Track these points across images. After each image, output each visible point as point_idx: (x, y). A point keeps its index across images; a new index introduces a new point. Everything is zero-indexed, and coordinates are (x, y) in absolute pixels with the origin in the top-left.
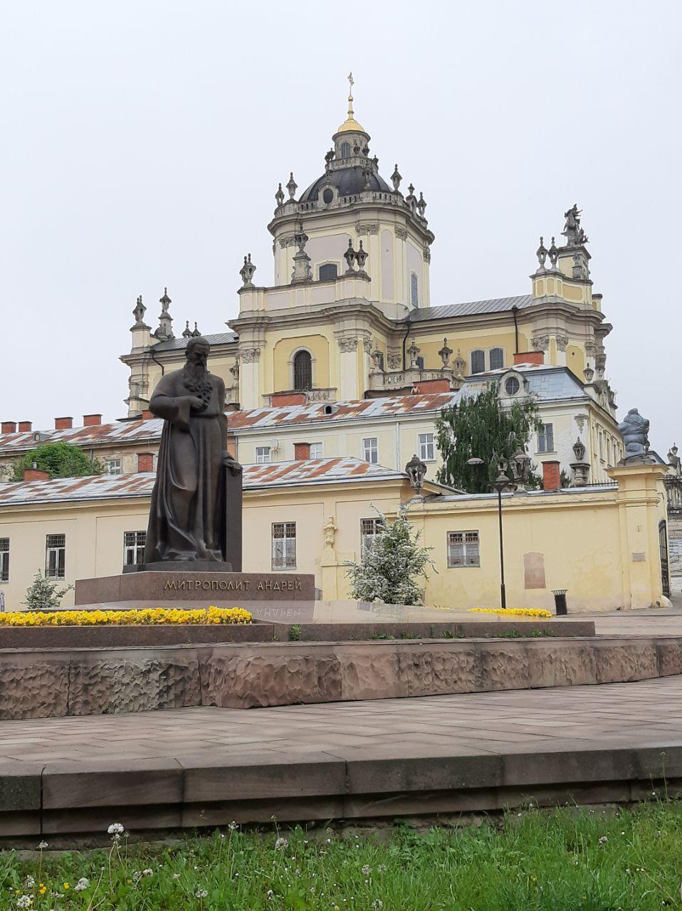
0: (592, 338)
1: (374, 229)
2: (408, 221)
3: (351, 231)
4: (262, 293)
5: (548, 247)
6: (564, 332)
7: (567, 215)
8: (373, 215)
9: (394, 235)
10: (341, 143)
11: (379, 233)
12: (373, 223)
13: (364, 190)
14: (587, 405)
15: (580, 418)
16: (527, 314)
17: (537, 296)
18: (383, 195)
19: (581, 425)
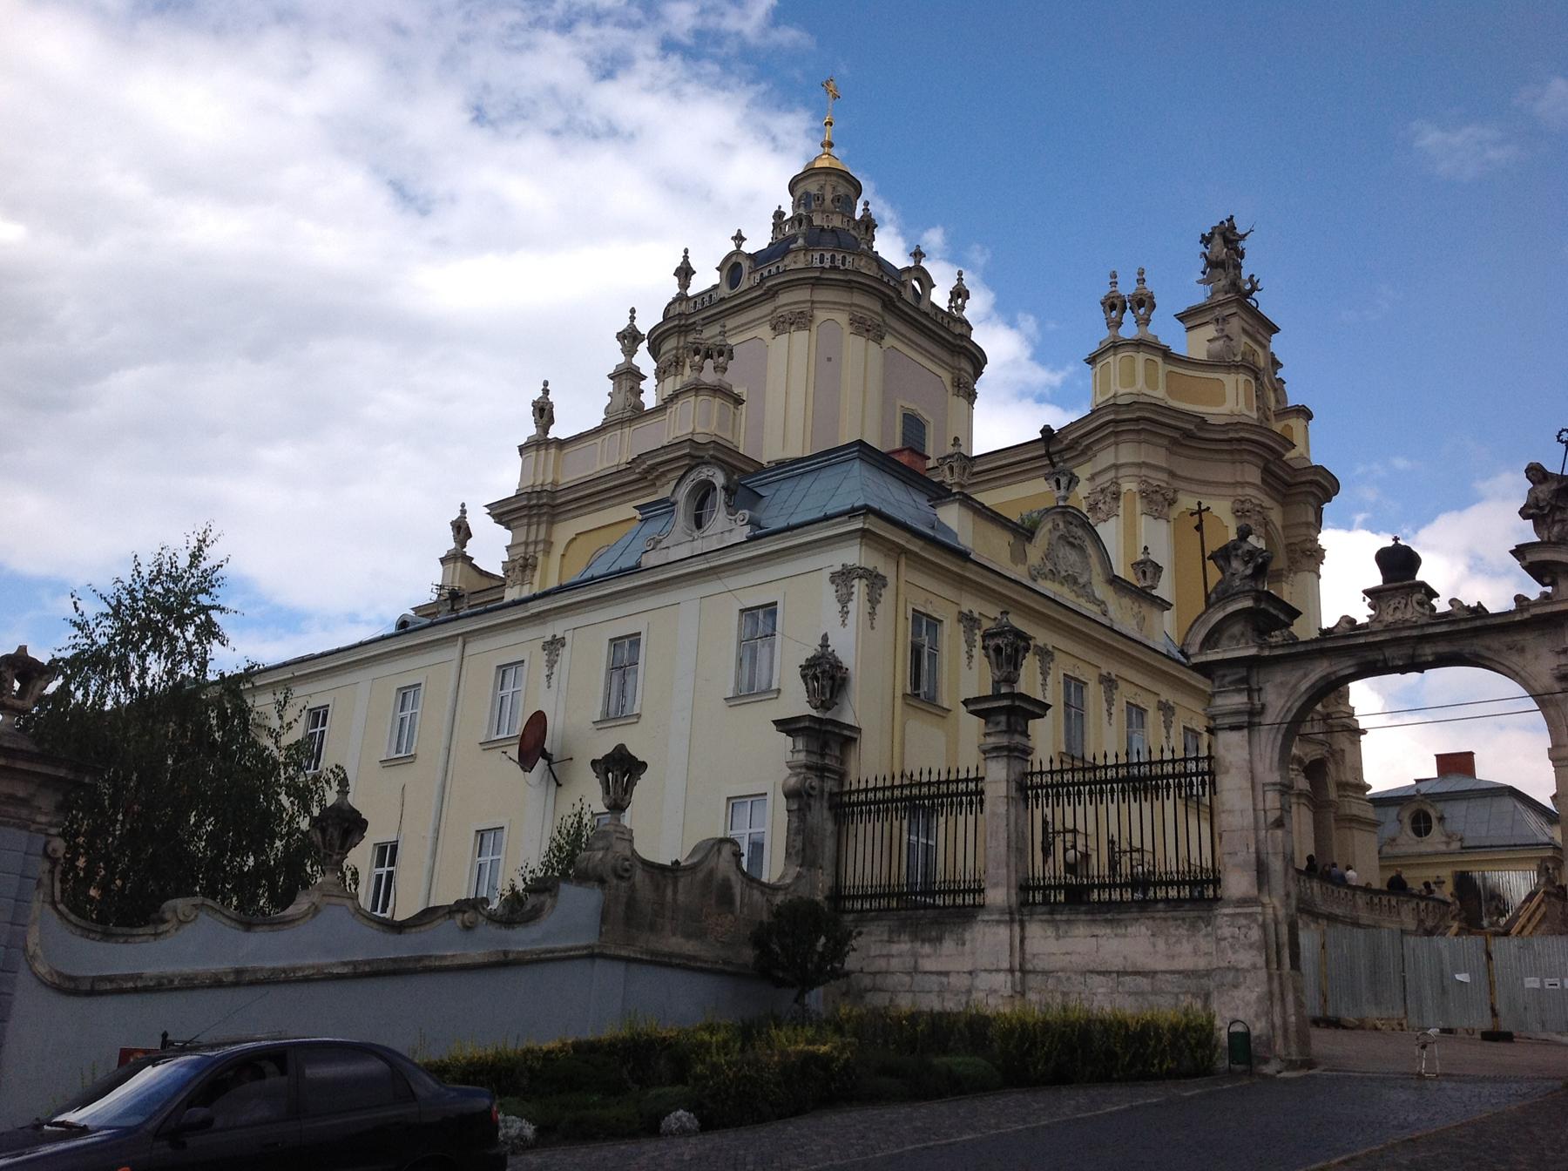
0: (1249, 491)
1: (801, 320)
2: (889, 305)
3: (765, 331)
4: (553, 451)
5: (1127, 288)
6: (1165, 477)
7: (1206, 240)
8: (802, 295)
9: (848, 329)
10: (798, 193)
11: (814, 328)
12: (805, 307)
13: (792, 251)
14: (863, 530)
15: (843, 577)
16: (1076, 441)
17: (1100, 400)
18: (828, 256)
19: (844, 601)
